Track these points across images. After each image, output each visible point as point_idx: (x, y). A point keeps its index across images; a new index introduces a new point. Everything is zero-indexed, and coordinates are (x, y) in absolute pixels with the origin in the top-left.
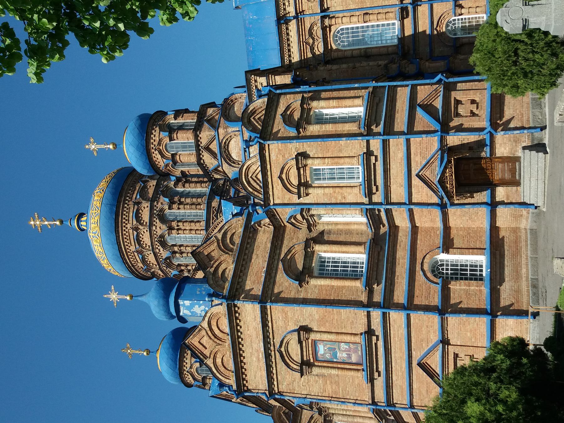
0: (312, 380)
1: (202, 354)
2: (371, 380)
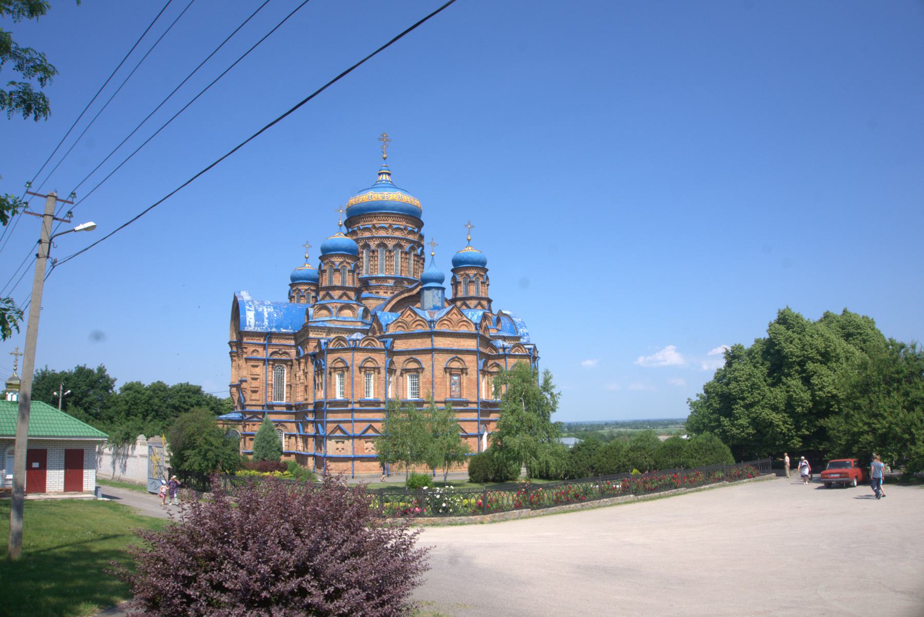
2: (445, 402)
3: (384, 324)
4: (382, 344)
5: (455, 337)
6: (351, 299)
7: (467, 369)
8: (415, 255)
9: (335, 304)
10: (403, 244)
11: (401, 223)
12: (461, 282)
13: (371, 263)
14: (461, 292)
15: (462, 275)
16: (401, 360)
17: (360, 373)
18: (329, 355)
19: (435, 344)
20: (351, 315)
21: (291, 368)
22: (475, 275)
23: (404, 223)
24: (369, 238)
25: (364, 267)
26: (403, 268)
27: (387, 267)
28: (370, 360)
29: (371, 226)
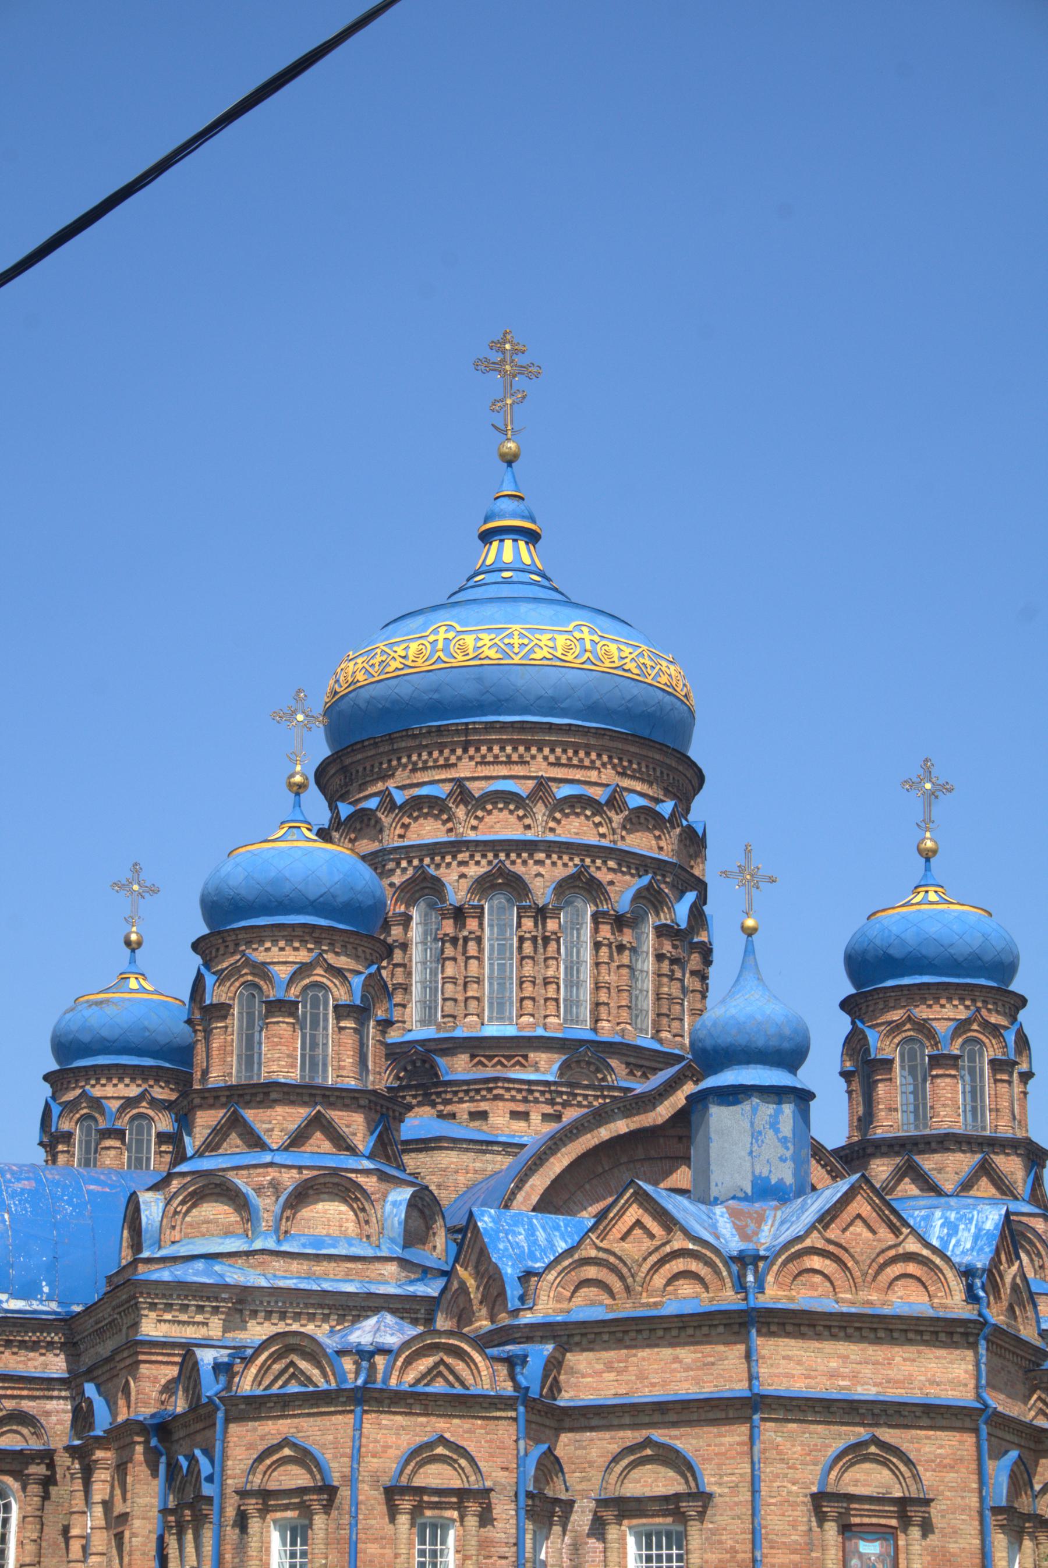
0: (796, 1513)
1: (832, 1220)
3: (510, 1271)
4: (503, 1370)
5: (863, 1339)
6: (352, 1150)
7: (927, 1502)
8: (662, 931)
9: (272, 1173)
10: (603, 876)
11: (593, 776)
12: (890, 1062)
13: (450, 970)
14: (891, 1110)
15: (896, 1028)
16: (594, 1453)
17: (393, 1514)
18: (233, 1428)
19: (763, 1370)
20: (351, 1227)
21: (46, 1497)
22: (962, 1026)
23: (608, 775)
24: (434, 850)
25: (416, 990)
26: (603, 997)
27: (528, 987)
28: (440, 1450)
29: (447, 788)
